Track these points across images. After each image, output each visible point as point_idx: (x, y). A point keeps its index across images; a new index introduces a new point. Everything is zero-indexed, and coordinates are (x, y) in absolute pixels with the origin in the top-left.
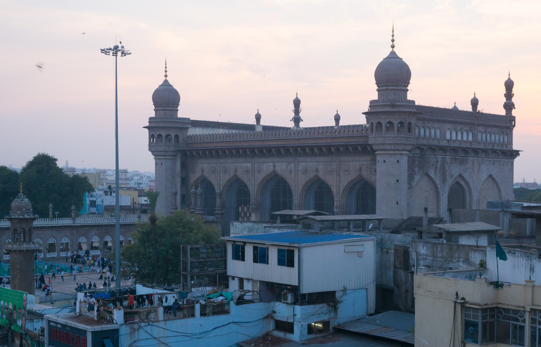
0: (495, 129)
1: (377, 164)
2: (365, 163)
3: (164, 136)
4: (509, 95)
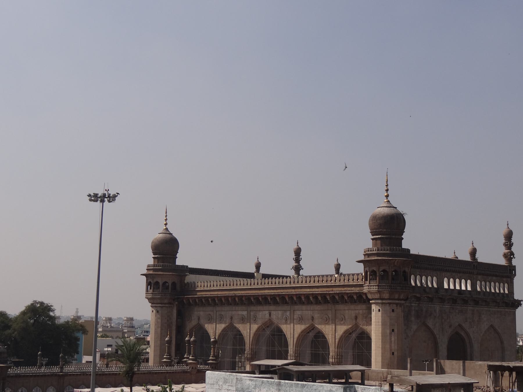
0: (494, 278)
1: (373, 314)
2: (361, 311)
3: (161, 284)
4: (509, 244)
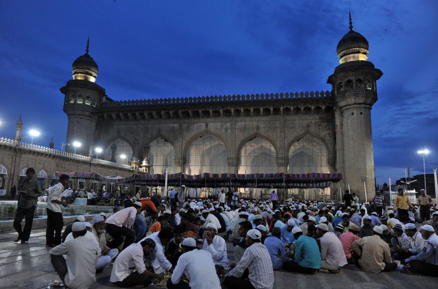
2: (313, 121)
